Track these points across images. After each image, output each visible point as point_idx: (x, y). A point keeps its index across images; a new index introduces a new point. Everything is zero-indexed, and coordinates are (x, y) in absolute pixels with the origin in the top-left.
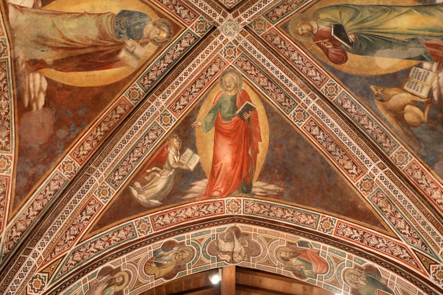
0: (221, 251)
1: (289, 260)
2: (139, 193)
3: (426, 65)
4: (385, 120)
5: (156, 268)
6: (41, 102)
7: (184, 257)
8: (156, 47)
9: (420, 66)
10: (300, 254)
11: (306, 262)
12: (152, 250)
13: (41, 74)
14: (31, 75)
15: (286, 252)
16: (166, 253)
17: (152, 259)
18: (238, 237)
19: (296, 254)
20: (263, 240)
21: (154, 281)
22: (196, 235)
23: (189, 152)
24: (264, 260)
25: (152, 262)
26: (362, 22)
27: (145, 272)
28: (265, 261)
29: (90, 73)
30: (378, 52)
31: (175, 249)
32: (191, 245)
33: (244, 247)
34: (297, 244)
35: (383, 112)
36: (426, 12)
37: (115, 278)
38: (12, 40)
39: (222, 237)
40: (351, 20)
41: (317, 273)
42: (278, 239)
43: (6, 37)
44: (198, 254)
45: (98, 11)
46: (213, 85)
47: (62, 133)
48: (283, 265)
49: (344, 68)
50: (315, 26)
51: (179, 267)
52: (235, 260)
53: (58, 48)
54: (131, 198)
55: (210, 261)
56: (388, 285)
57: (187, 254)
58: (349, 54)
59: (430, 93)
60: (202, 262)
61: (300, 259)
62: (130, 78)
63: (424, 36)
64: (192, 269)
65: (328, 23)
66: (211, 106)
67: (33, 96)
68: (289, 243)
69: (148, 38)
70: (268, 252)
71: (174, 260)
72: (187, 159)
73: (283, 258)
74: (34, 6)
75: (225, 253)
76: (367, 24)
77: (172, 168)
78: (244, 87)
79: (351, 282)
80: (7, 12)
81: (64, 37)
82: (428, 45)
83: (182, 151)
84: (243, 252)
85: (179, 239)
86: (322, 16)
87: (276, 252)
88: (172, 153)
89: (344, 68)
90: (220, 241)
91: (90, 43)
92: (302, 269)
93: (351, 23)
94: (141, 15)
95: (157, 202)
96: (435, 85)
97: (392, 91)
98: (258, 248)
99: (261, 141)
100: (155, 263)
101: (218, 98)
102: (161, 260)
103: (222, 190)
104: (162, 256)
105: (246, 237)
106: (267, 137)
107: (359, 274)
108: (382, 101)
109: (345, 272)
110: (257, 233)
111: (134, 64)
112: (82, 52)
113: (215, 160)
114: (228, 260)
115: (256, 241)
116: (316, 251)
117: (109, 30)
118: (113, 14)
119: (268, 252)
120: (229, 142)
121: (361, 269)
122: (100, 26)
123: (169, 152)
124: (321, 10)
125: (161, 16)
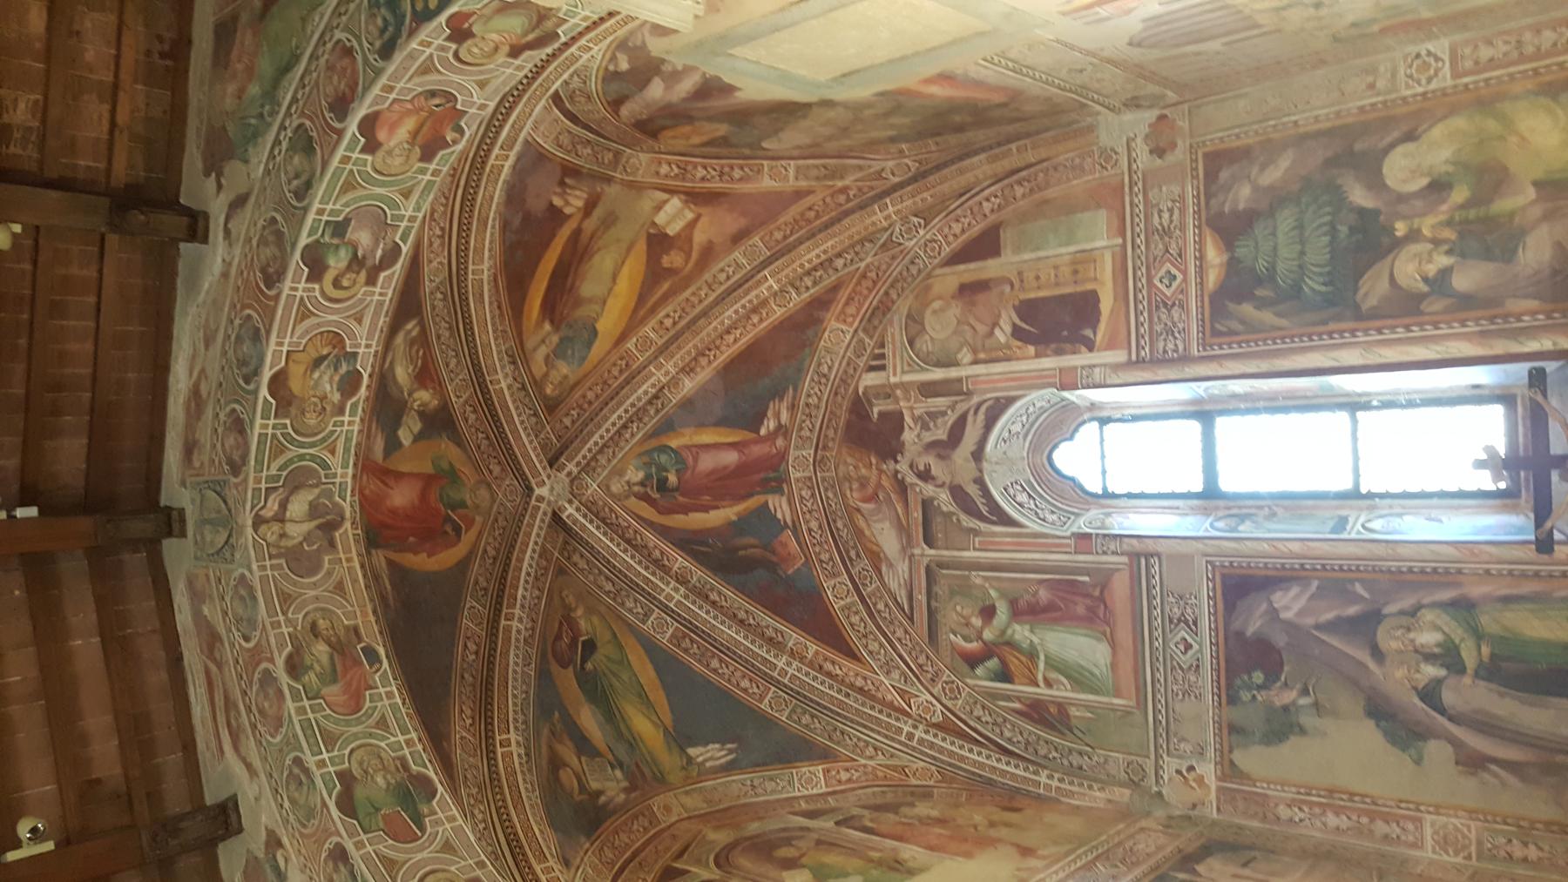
0: (291, 493)
1: (316, 636)
2: (410, 332)
3: (618, 773)
4: (540, 746)
5: (314, 355)
6: (557, 201)
7: (308, 415)
8: (538, 378)
9: (613, 767)
10: (342, 653)
11: (334, 670)
12: (361, 351)
13: (579, 209)
14: (585, 196)
15: (333, 628)
16: (337, 378)
17: (344, 347)
18: (319, 527)
19: (340, 648)
20: (335, 578)
21: (285, 349)
22: (348, 440)
23: (417, 426)
24: (288, 588)
25: (334, 347)
26: (614, 675)
27: (322, 333)
28: (286, 590)
29: (548, 276)
30: (593, 707)
31: (336, 397)
32: (330, 428)
33: (301, 543)
34: (362, 645)
35: (544, 740)
36: (668, 743)
37: (358, 273)
38: (631, 185)
39: (329, 494)
40: (608, 658)
41: (323, 698)
42: (352, 606)
43: (639, 179)
44: (302, 445)
45: (610, 302)
46: (478, 469)
47: (517, 222)
48: (299, 628)
49: (555, 668)
50: (580, 612)
51: (289, 404)
52: (263, 528)
53: (592, 237)
54: (407, 319)
55: (274, 472)
56: (427, 820)
57: (312, 422)
58: (571, 669)
59: (599, 793)
60: (279, 450)
61: (332, 658)
62: (520, 334)
63: (643, 755)
64: (270, 431)
65: (590, 629)
66: (457, 465)
67: (568, 191)
68: (356, 630)
69: (553, 367)
70: (312, 593)
71: (311, 392)
72: (411, 423)
73: (314, 626)
74: (654, 224)
75: (283, 506)
76: (614, 680)
77: (410, 395)
78: (479, 519)
79: (361, 764)
80: (664, 191)
81: (599, 249)
82: (637, 766)
83: (422, 415)
84: (290, 543)
85: (354, 406)
86: (595, 620)
87: (323, 609)
88: (424, 396)
89: (555, 668)
90: (317, 491)
91: (577, 283)
92: (311, 667)
93: (604, 660)
94: (583, 359)
95: (387, 365)
96: (610, 793)
97: (569, 743)
98: (313, 571)
99: (429, 556)
100: (329, 354)
101: (464, 478)
102: (329, 366)
103: (367, 492)
104: (336, 369)
105: (325, 543)
106: (436, 567)
107: (393, 769)
108: (553, 734)
109: (370, 745)
110: (345, 564)
111: (529, 344)
112: (573, 269)
113: (399, 476)
114: (262, 513)
115: (326, 565)
116: (371, 682)
117: (583, 312)
118: (596, 320)
119: (312, 593)
120: (416, 502)
121: (406, 767)
122: (590, 300)
123: (426, 388)
124: (603, 617)
125: (573, 388)
